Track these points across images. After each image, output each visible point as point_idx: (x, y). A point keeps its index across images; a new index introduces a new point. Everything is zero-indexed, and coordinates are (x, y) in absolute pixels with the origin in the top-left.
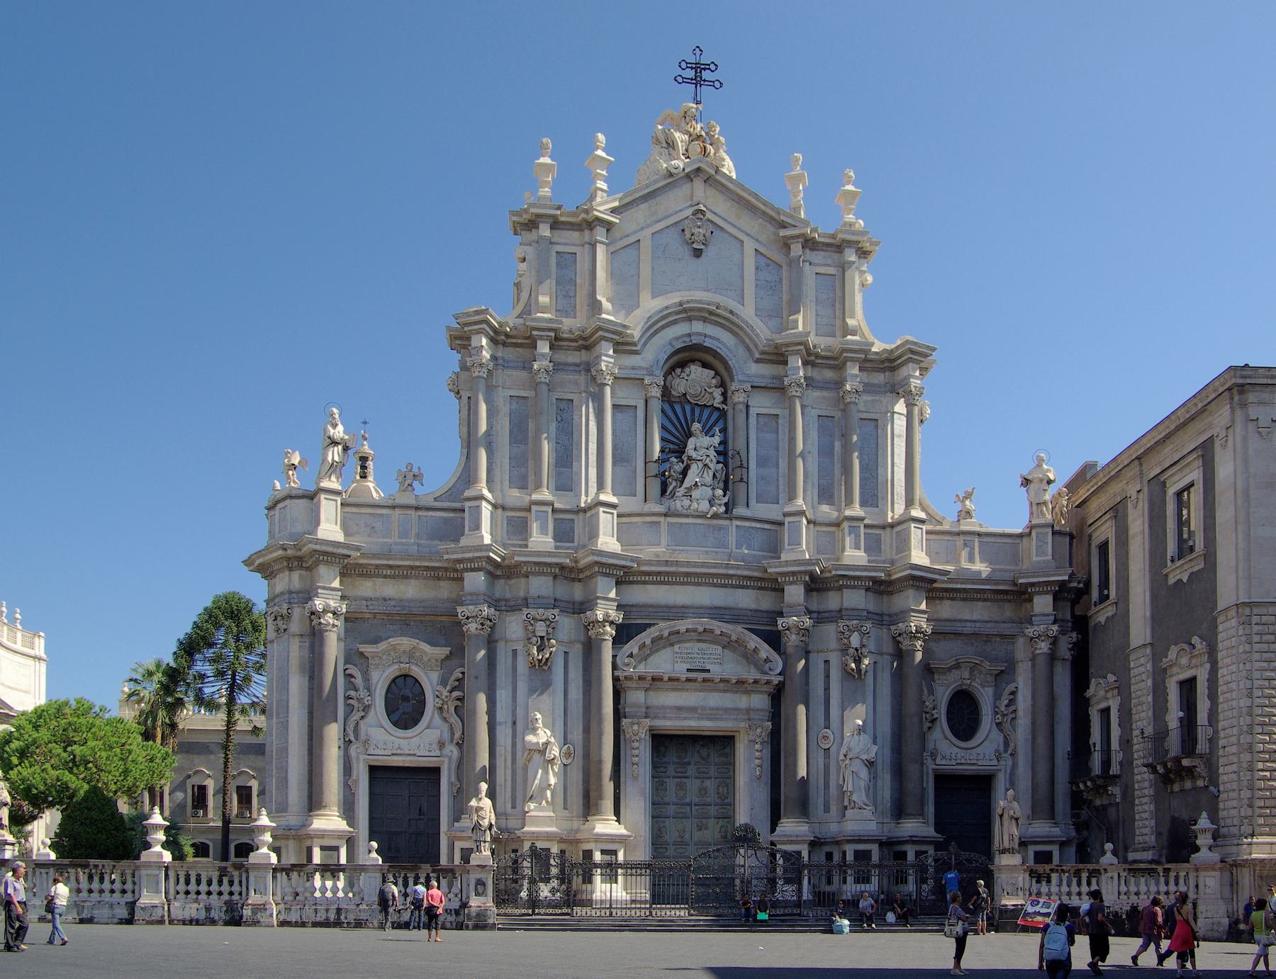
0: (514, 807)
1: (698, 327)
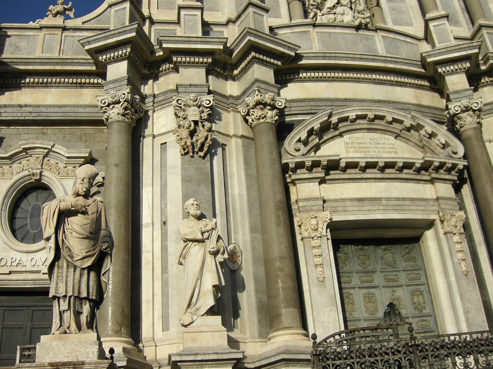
0: (165, 328)
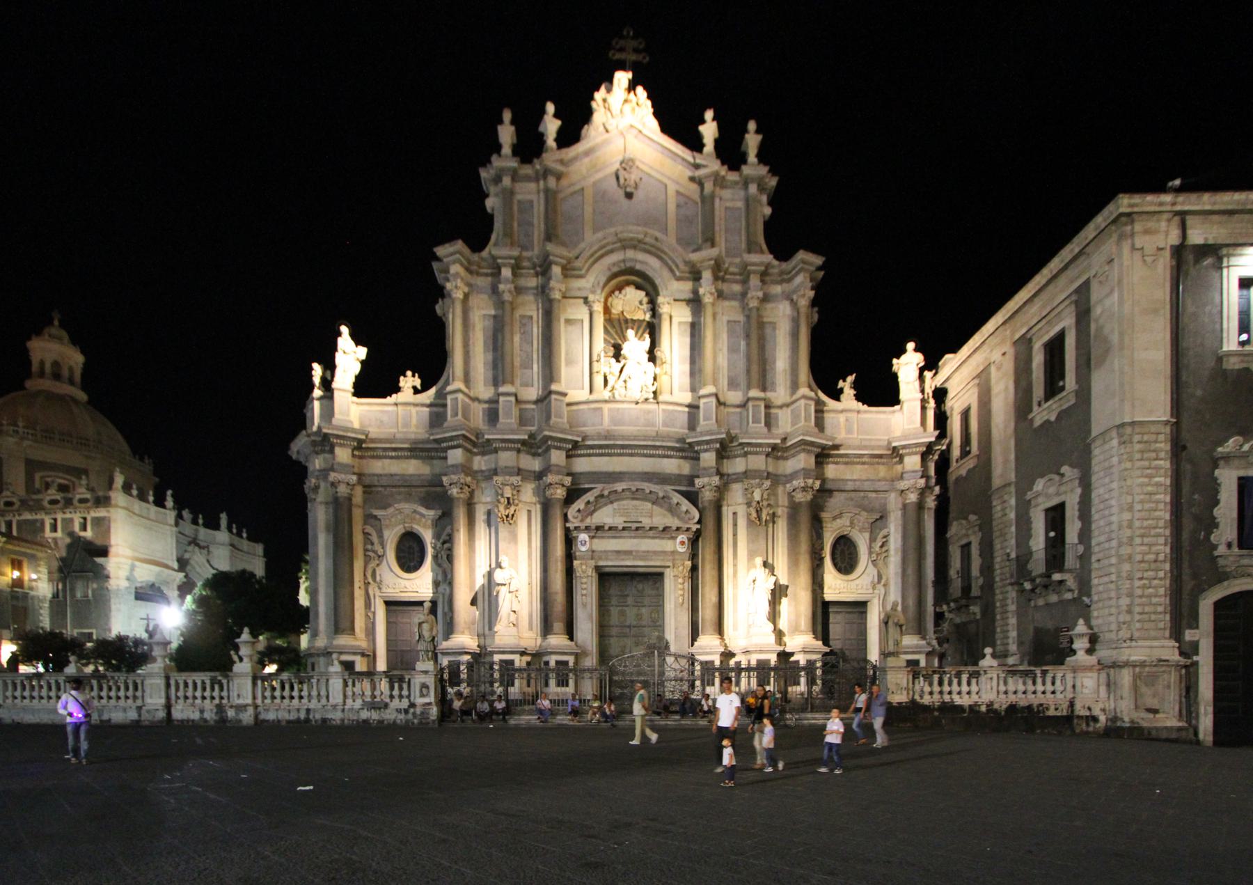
1: (630, 254)
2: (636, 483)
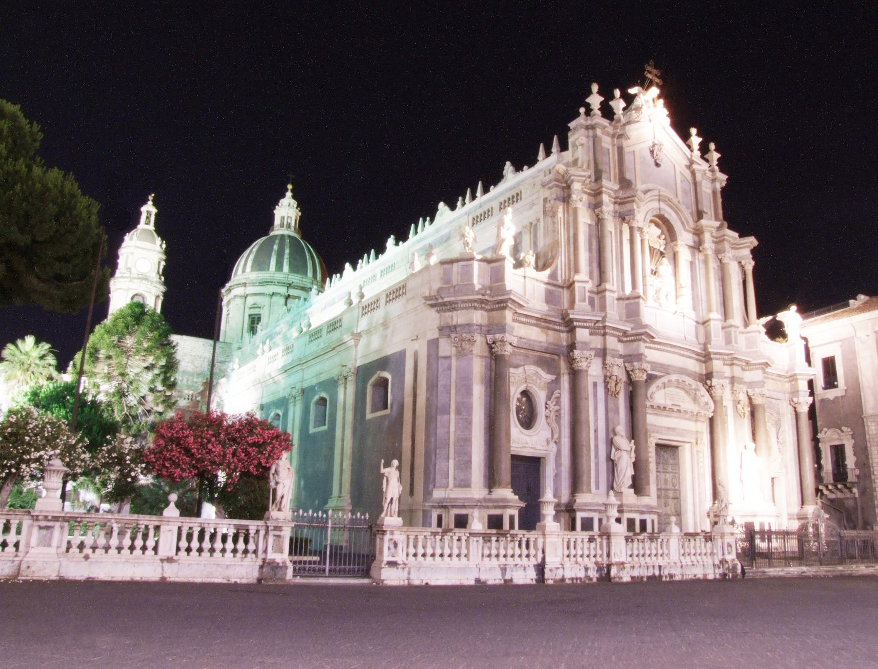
0: (597, 487)
2: (683, 376)
